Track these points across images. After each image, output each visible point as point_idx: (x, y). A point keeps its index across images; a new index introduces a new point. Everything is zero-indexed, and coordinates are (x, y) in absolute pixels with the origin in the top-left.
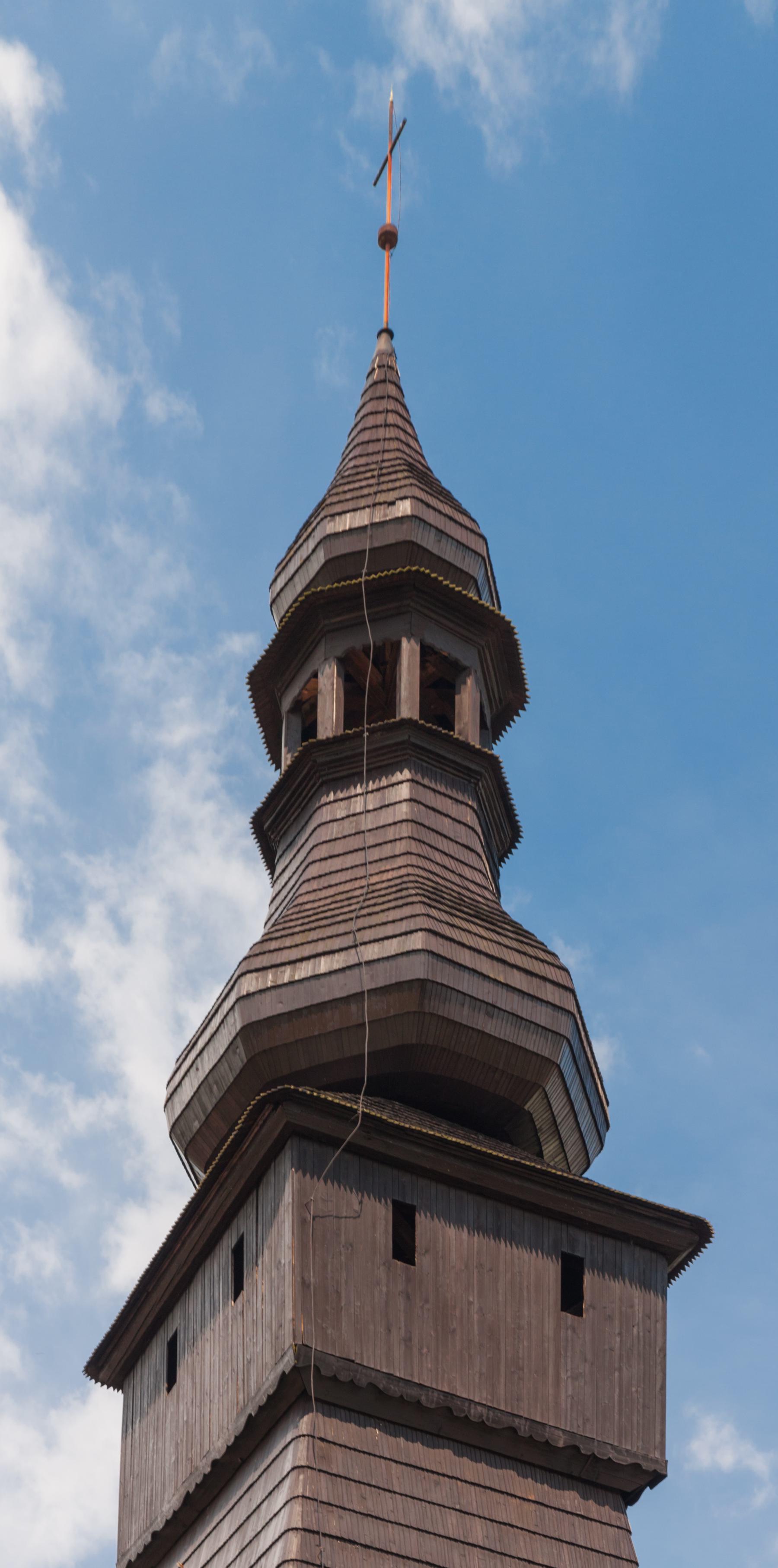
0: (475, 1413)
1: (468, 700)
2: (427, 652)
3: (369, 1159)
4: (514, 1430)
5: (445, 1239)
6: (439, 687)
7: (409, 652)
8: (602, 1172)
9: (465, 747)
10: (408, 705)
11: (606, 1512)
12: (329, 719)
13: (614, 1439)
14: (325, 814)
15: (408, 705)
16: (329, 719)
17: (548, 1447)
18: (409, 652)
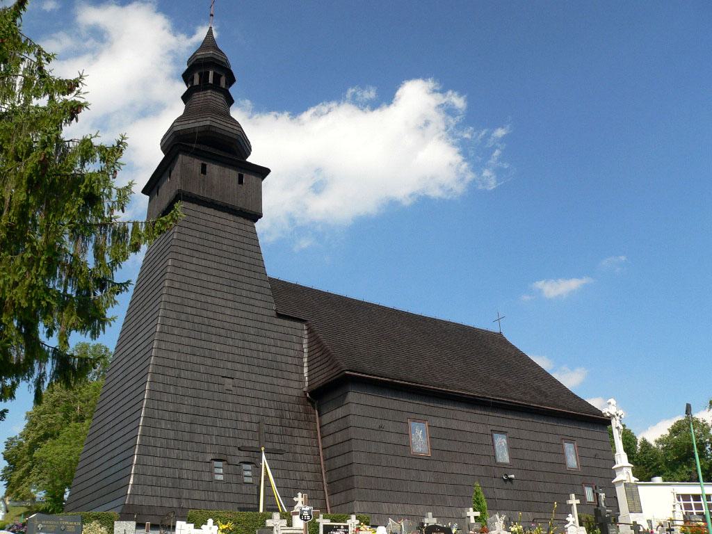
0: (219, 203)
2: (214, 74)
3: (196, 154)
4: (227, 207)
5: (214, 169)
7: (211, 73)
8: (249, 160)
10: (211, 81)
11: (249, 222)
12: (196, 82)
13: (252, 209)
14: (194, 97)
15: (211, 81)
16: (196, 82)
17: (235, 210)
18: (211, 73)
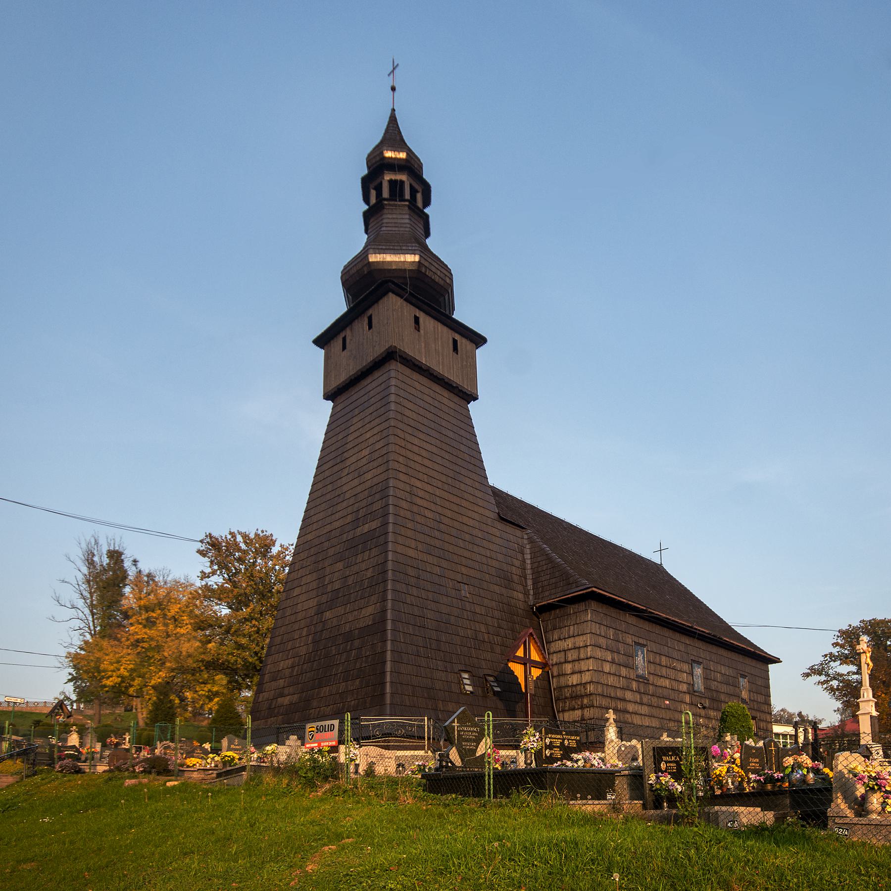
1: (419, 196)
6: (413, 192)
9: (418, 208)
